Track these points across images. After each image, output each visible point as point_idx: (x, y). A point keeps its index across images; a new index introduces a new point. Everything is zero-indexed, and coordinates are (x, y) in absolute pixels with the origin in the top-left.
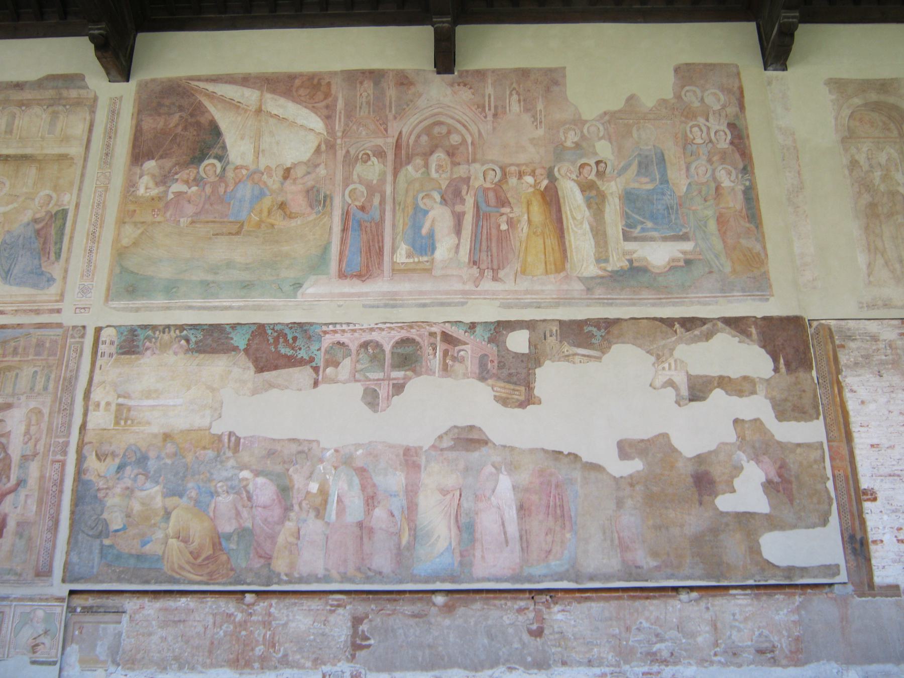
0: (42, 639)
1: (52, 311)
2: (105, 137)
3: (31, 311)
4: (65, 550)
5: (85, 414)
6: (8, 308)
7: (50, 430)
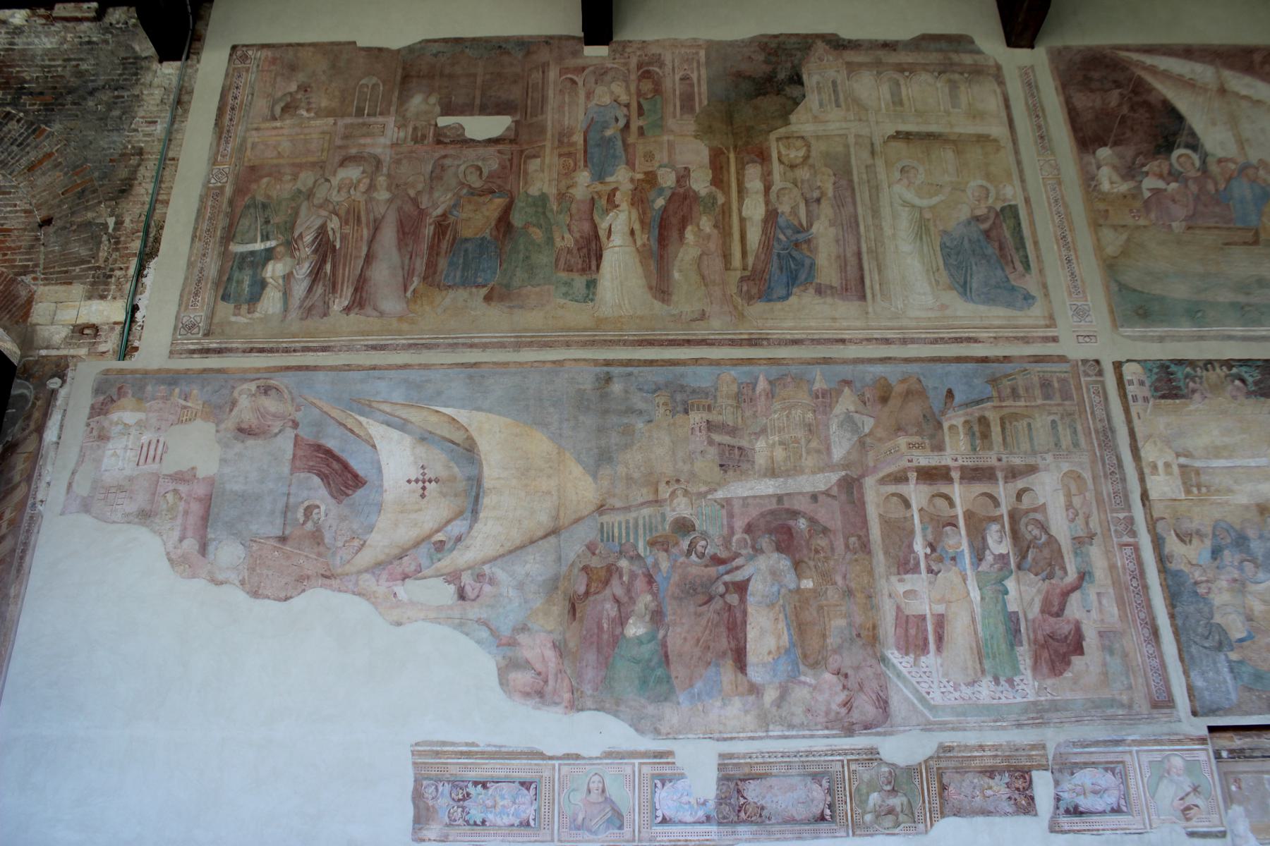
0: (1192, 800)
1: (1046, 339)
2: (1030, 115)
3: (1016, 338)
4: (1181, 669)
5: (1142, 480)
6: (983, 335)
7: (1100, 501)
